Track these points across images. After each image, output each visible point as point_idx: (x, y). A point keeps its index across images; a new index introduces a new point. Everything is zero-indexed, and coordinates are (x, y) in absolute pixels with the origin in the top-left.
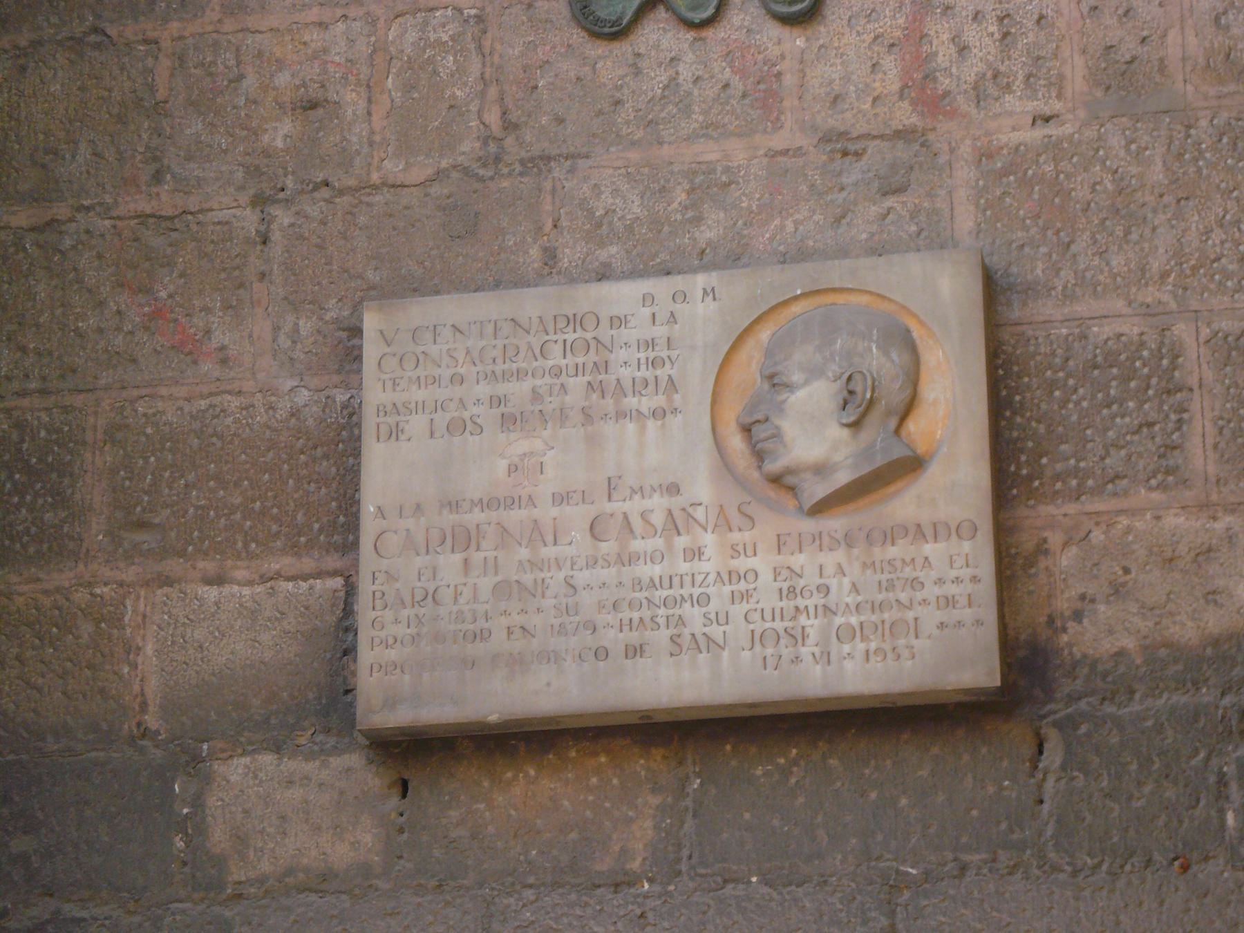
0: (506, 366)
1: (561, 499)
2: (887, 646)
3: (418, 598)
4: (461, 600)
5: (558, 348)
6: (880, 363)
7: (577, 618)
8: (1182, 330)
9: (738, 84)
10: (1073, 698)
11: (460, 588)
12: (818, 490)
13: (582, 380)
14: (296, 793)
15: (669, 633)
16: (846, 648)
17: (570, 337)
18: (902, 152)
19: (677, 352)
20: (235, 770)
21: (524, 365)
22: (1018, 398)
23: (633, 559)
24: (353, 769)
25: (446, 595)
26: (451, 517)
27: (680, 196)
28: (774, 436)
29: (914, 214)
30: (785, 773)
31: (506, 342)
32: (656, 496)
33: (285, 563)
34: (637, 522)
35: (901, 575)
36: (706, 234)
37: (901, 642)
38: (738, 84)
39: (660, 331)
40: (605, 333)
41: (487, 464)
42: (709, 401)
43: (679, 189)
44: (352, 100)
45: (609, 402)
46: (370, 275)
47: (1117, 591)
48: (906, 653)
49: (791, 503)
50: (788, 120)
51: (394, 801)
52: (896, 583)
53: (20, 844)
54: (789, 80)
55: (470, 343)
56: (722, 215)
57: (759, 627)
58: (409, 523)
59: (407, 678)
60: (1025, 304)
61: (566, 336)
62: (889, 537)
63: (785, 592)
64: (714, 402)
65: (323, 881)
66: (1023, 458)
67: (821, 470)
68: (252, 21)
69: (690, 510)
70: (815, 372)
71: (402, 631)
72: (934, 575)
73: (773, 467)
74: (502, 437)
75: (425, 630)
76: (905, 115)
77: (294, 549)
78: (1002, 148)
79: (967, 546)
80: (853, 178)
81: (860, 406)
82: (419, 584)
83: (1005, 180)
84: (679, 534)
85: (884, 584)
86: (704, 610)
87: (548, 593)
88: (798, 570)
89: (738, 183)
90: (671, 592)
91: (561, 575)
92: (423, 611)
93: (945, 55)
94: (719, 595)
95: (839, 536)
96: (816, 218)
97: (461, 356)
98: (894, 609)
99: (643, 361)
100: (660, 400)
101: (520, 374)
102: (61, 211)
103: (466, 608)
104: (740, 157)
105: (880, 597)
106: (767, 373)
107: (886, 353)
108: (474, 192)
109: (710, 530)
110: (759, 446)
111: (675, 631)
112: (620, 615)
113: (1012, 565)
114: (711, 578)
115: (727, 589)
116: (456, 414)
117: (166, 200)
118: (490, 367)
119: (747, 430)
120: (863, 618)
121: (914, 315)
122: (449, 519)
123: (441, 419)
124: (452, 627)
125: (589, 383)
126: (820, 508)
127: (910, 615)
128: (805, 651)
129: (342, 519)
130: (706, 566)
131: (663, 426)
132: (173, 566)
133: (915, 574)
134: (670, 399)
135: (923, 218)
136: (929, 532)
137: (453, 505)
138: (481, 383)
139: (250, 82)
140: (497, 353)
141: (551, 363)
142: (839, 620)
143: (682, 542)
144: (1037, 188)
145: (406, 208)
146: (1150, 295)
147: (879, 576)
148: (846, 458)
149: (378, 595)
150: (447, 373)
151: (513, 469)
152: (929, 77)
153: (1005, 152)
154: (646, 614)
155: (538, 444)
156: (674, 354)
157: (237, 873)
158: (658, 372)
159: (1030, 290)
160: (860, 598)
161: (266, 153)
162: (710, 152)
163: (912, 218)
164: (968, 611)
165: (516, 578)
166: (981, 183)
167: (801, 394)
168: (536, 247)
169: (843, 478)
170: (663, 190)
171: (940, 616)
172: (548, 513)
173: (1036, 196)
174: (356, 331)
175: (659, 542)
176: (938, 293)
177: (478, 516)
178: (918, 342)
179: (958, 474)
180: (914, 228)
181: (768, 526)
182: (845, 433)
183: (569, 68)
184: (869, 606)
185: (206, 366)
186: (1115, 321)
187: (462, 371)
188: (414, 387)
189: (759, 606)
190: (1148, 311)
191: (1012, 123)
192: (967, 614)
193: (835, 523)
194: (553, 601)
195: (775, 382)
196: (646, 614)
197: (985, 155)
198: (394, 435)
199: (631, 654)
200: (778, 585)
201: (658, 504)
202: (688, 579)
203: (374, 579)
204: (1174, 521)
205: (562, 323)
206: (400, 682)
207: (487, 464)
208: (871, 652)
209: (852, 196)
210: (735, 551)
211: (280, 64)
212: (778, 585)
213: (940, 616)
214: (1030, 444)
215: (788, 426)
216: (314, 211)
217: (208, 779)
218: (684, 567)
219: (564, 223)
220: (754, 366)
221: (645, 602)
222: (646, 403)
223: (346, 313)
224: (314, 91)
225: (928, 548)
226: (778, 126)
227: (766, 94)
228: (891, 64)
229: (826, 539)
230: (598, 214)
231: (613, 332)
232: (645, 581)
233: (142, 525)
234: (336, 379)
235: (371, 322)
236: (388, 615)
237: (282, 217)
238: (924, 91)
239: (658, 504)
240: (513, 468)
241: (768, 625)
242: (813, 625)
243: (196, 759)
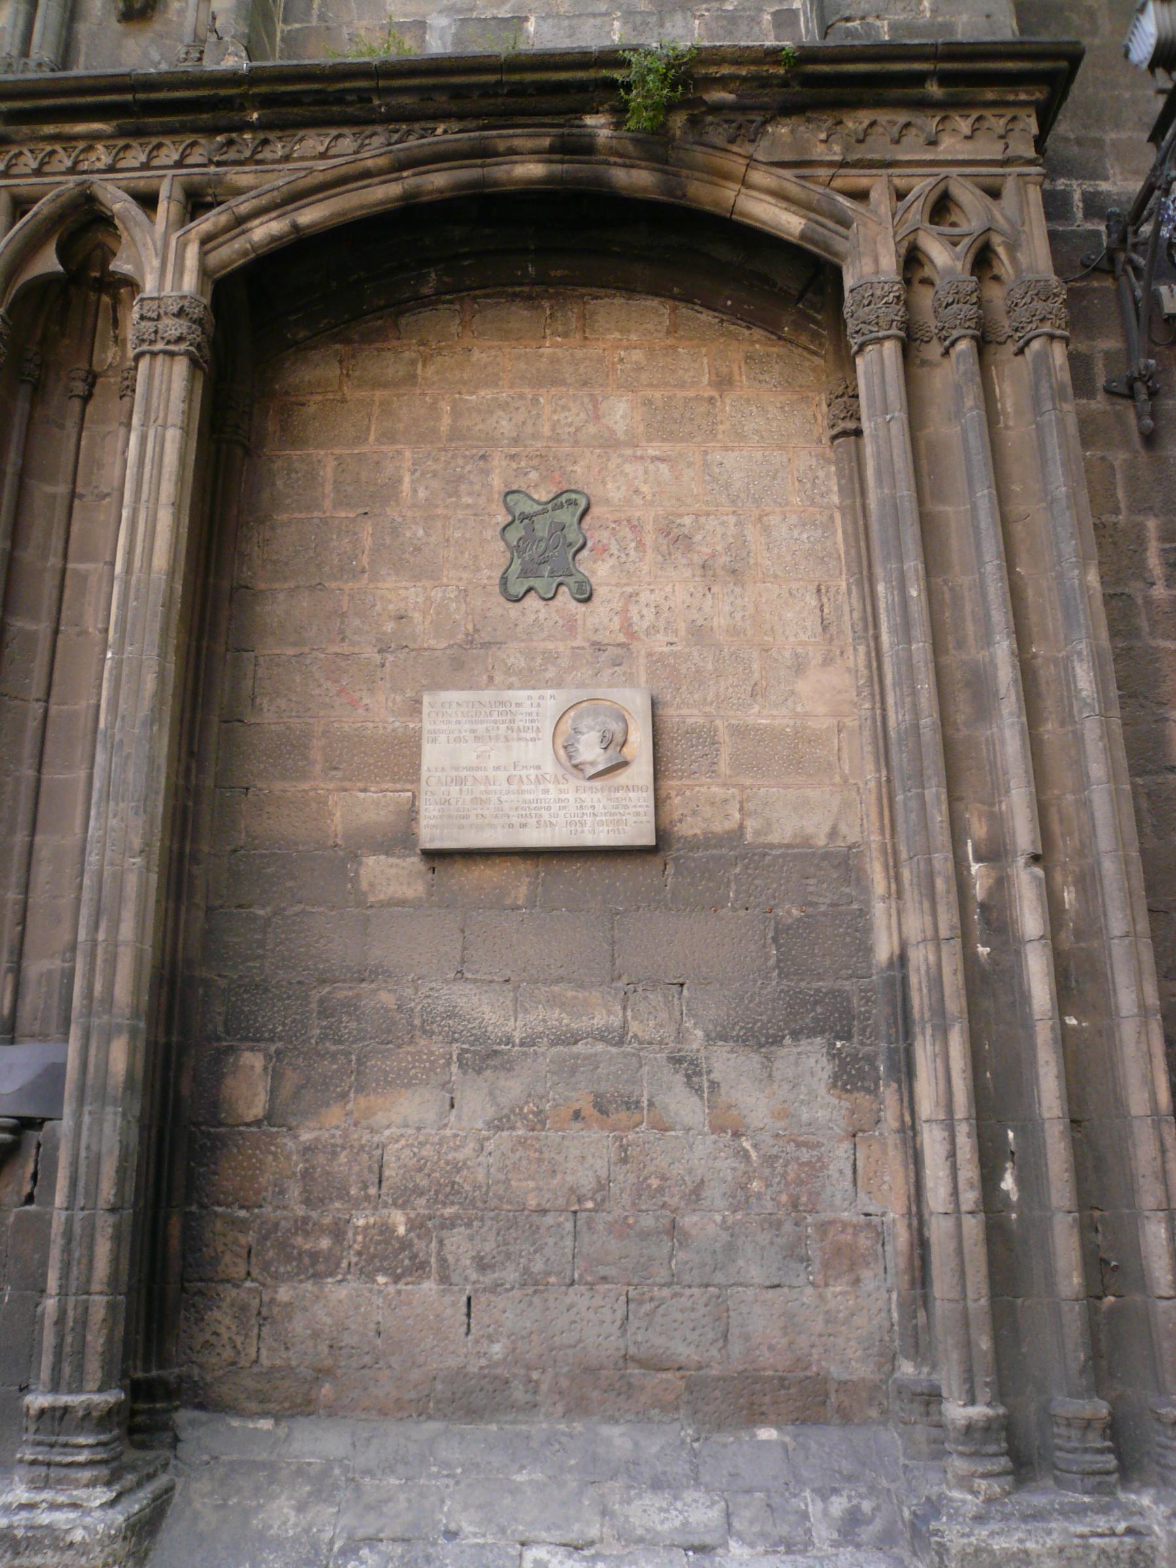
1: (497, 768)
6: (616, 727)
8: (718, 722)
9: (561, 622)
10: (678, 850)
12: (592, 771)
14: (393, 871)
18: (619, 651)
20: (371, 861)
23: (523, 792)
24: (415, 862)
25: (453, 801)
27: (539, 661)
30: (575, 872)
33: (389, 785)
36: (549, 675)
38: (561, 622)
39: (534, 710)
40: (513, 709)
41: (468, 754)
44: (417, 616)
47: (694, 813)
49: (580, 774)
50: (579, 636)
51: (430, 875)
53: (289, 884)
54: (580, 622)
62: (617, 789)
65: (402, 903)
67: (592, 764)
68: (380, 585)
70: (592, 728)
71: (436, 813)
76: (622, 638)
77: (394, 781)
93: (636, 618)
94: (555, 807)
98: (615, 814)
100: (534, 735)
101: (482, 722)
102: (306, 650)
104: (561, 649)
113: (659, 802)
117: (345, 648)
119: (565, 747)
122: (454, 774)
126: (591, 778)
132: (347, 784)
137: (457, 769)
139: (378, 607)
143: (541, 787)
146: (707, 709)
152: (630, 625)
157: (371, 899)
159: (665, 704)
161: (384, 634)
162: (550, 646)
169: (601, 767)
172: (491, 773)
174: (419, 702)
175: (532, 787)
176: (636, 702)
177: (465, 773)
179: (641, 770)
181: (574, 782)
183: (499, 611)
185: (361, 711)
186: (695, 718)
190: (707, 715)
191: (659, 644)
193: (597, 783)
195: (576, 731)
197: (649, 655)
201: (533, 773)
204: (714, 789)
206: (434, 831)
207: (468, 754)
211: (390, 601)
215: (581, 747)
216: (402, 656)
217: (360, 864)
222: (529, 735)
224: (402, 612)
225: (631, 794)
226: (575, 638)
227: (571, 626)
228: (616, 619)
233: (336, 768)
235: (426, 699)
237: (390, 658)
238: (628, 628)
239: (533, 773)
242: (589, 820)
243: (356, 856)
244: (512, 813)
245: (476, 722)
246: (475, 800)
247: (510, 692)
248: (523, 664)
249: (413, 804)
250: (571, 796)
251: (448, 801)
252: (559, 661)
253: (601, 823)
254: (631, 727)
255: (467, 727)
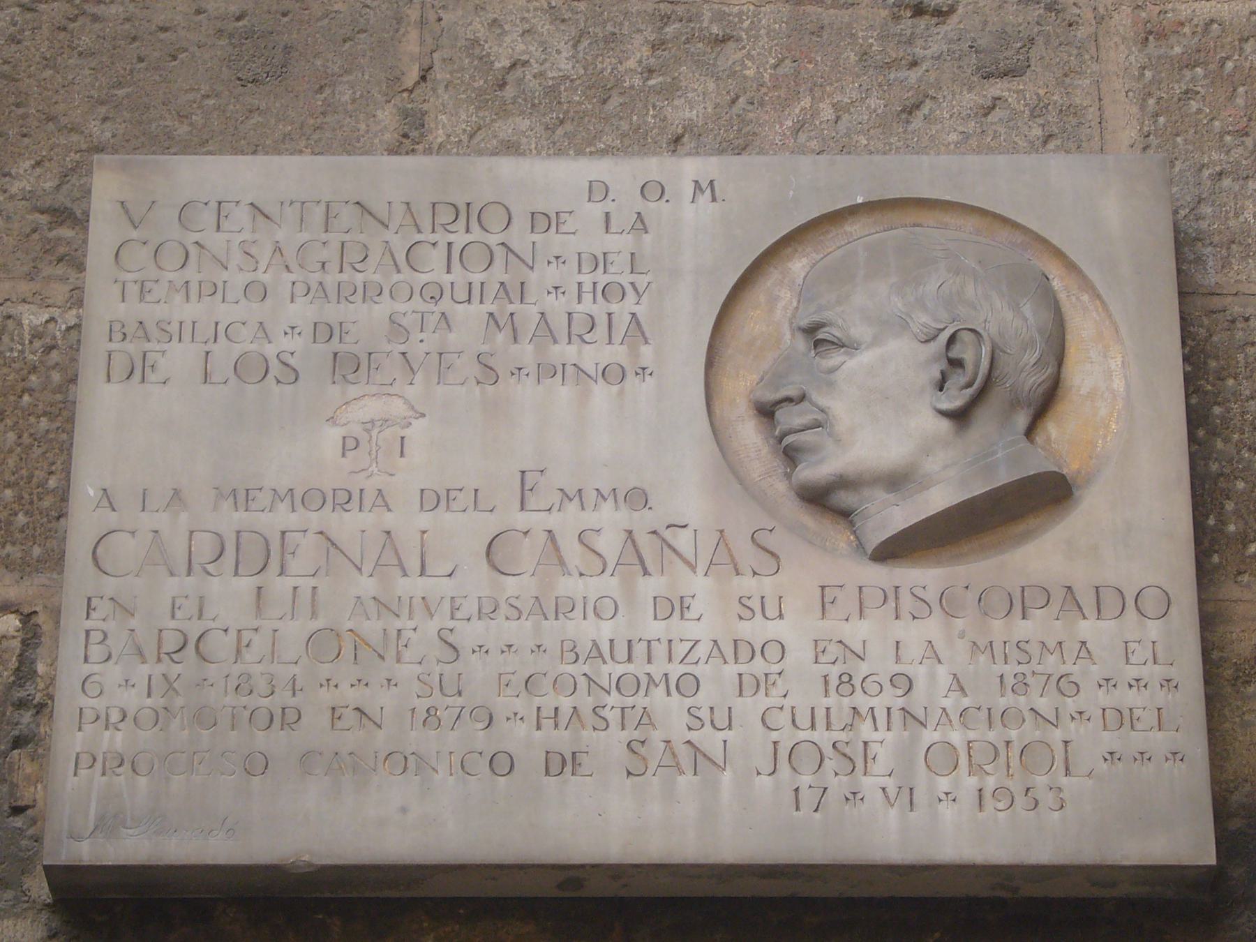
0: (344, 277)
1: (437, 499)
2: (1016, 786)
3: (170, 646)
4: (248, 656)
5: (439, 255)
6: (1005, 319)
7: (459, 701)
11: (246, 636)
12: (894, 516)
13: (478, 310)
15: (625, 736)
16: (944, 784)
17: (460, 239)
19: (647, 278)
21: (377, 277)
22: (1217, 410)
23: (563, 608)
25: (221, 645)
26: (236, 515)
27: (638, 52)
28: (817, 425)
29: (1037, 111)
31: (347, 237)
32: (608, 506)
34: (572, 552)
35: (1039, 669)
36: (682, 113)
37: (1041, 780)
39: (619, 243)
40: (520, 237)
42: (703, 360)
43: (638, 39)
45: (526, 352)
46: (94, 127)
48: (1048, 799)
49: (841, 538)
52: (1029, 680)
55: (280, 235)
56: (711, 86)
57: (787, 738)
58: (162, 520)
59: (142, 781)
60: (1225, 264)
61: (452, 238)
62: (1020, 603)
63: (834, 681)
64: (710, 364)
66: (1230, 506)
67: (897, 481)
69: (667, 534)
71: (133, 699)
72: (1096, 672)
73: (814, 471)
74: (334, 392)
75: (179, 702)
78: (1182, 24)
79: (1154, 629)
80: (935, 49)
81: (969, 385)
82: (173, 624)
83: (1188, 74)
84: (646, 572)
85: (1010, 681)
86: (689, 702)
87: (407, 655)
88: (858, 648)
89: (739, 40)
90: (630, 668)
91: (432, 626)
92: (177, 669)
95: (931, 595)
96: (873, 102)
97: (264, 255)
99: (587, 287)
100: (617, 353)
101: (370, 293)
103: (257, 669)
105: (1003, 703)
106: (804, 323)
107: (1016, 308)
108: (284, 15)
109: (701, 569)
110: (789, 439)
111: (636, 735)
112: (537, 701)
114: (702, 650)
115: (731, 670)
116: (253, 347)
118: (317, 276)
119: (766, 412)
120: (972, 735)
121: (1058, 254)
122: (229, 520)
123: (224, 354)
124: (229, 700)
125: (491, 314)
127: (1057, 735)
128: (869, 784)
129: (21, 519)
130: (693, 630)
131: (621, 393)
133: (1064, 669)
134: (634, 353)
135: (1052, 117)
136: (1088, 602)
137: (242, 497)
138: (300, 300)
140: (331, 254)
141: (424, 278)
142: (929, 736)
143: (650, 586)
144: (1241, 90)
145: (164, 29)
147: (999, 668)
148: (946, 467)
149: (96, 637)
150: (241, 279)
151: (349, 445)
153: (1187, 30)
154: (586, 702)
155: (397, 408)
156: (641, 281)
158: (614, 308)
160: (966, 702)
163: (1033, 116)
164: (1160, 735)
165: (349, 625)
166: (1148, 74)
167: (866, 358)
168: (389, 109)
170: (611, 39)
171: (1109, 740)
172: (409, 521)
173: (1240, 101)
174: (71, 216)
175: (610, 584)
177: (284, 517)
178: (1062, 296)
180: (1037, 132)
182: (945, 425)
184: (983, 714)
187: (266, 278)
188: (179, 298)
189: (787, 703)
192: (1159, 741)
194: (418, 669)
196: (586, 702)
198: (138, 373)
199: (555, 769)
200: (823, 669)
201: (610, 522)
202: (660, 650)
203: (89, 608)
205: (445, 216)
208: (987, 794)
209: (932, 77)
210: (746, 608)
212: (823, 669)
213: (1109, 740)
214: (1240, 485)
215: (841, 406)
218: (655, 629)
219: (439, 74)
220: (779, 313)
221: (582, 682)
222: (593, 356)
223: (48, 185)
225: (1087, 628)
229: (907, 602)
230: (497, 65)
231: (536, 237)
232: (585, 647)
234: (24, 288)
235: (107, 187)
236: (114, 672)
239: (610, 522)
240: (351, 443)
241: (802, 735)
242: (885, 743)
244: (504, 704)
245: (343, 294)
246: (326, 643)
247: (507, 166)
248: (564, 64)
249: (24, 672)
250: (794, 630)
251: (195, 646)
252: (732, 54)
253: (945, 759)
254: (1083, 326)
255: (302, 312)
